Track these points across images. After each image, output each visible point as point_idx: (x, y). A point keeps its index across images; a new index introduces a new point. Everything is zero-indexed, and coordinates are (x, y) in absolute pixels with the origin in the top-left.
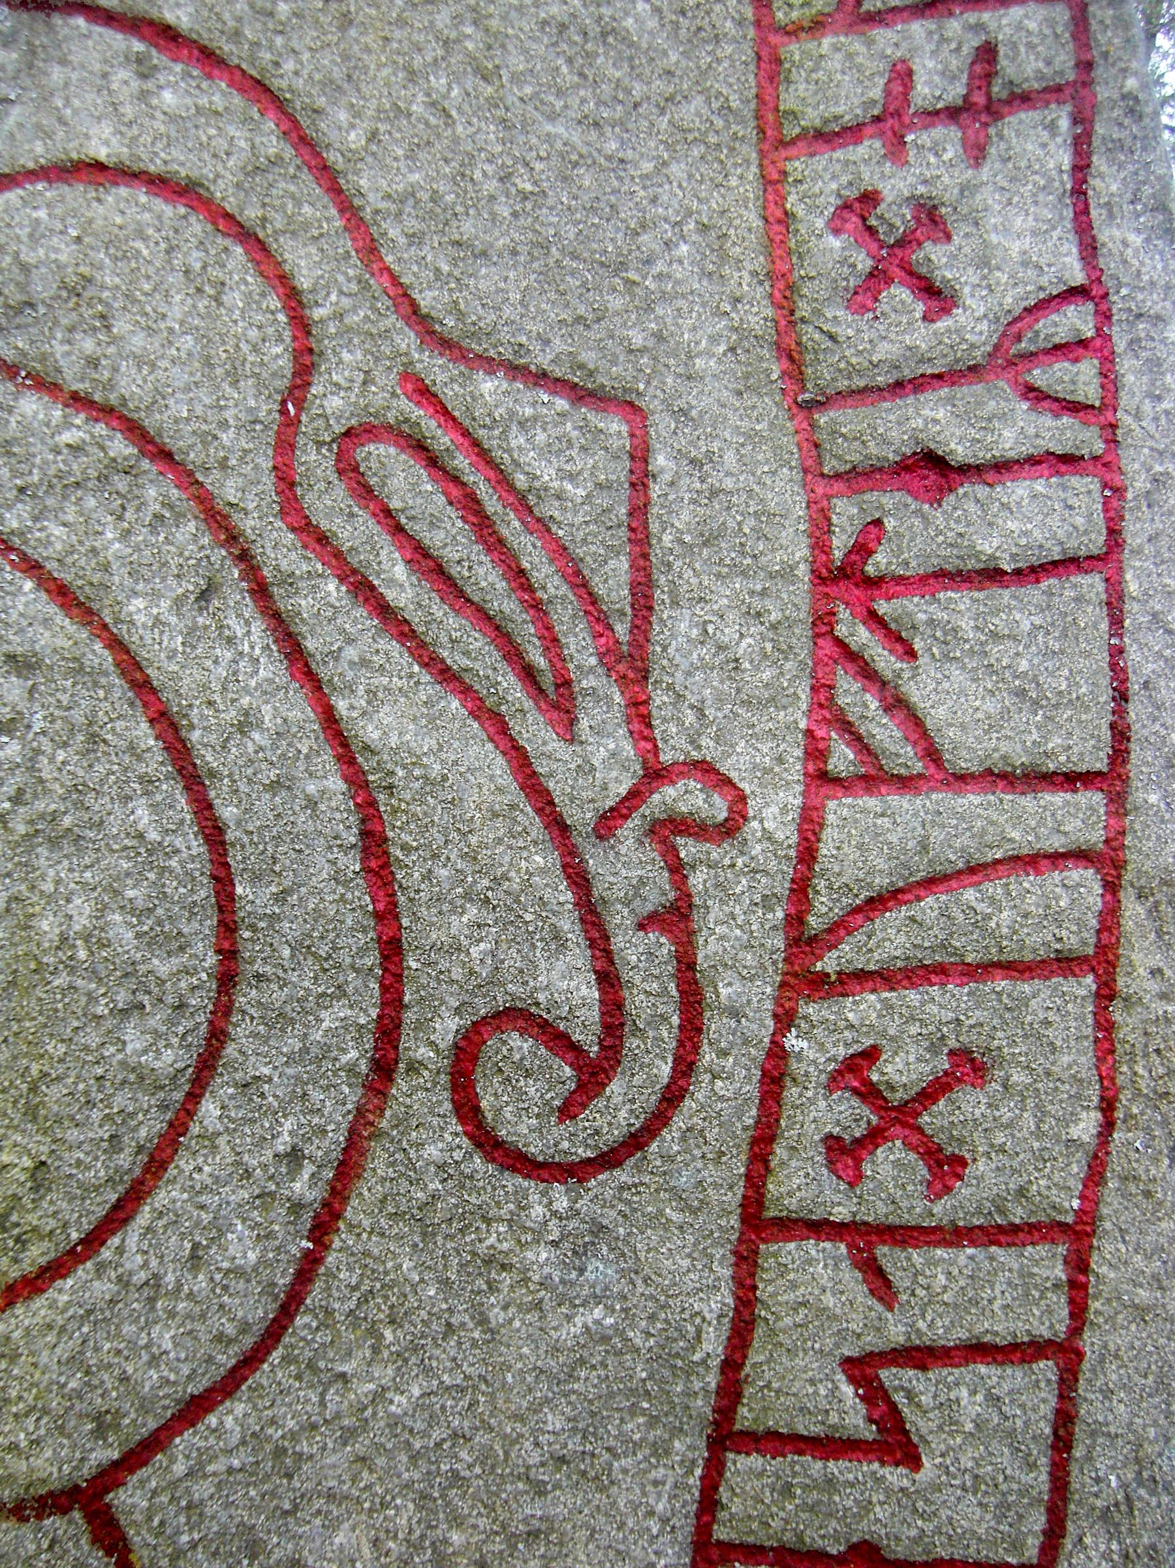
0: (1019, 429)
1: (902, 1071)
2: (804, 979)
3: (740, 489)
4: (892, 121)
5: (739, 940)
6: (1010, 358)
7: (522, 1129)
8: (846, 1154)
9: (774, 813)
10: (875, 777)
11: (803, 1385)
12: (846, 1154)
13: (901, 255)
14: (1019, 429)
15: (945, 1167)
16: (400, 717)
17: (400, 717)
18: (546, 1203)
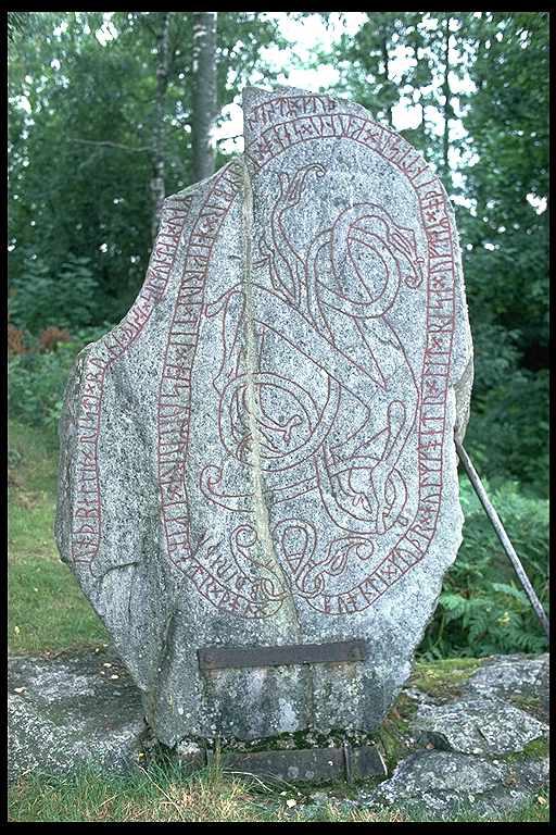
0: (443, 229)
1: (439, 278)
2: (429, 273)
3: (420, 234)
4: (430, 206)
5: (425, 270)
6: (441, 223)
7: (411, 284)
8: (435, 285)
9: (426, 261)
10: (434, 257)
11: (434, 303)
12: (435, 285)
13: (432, 216)
14: (443, 229)
15: (443, 285)
16: (398, 255)
17: (398, 255)
18: (413, 291)
